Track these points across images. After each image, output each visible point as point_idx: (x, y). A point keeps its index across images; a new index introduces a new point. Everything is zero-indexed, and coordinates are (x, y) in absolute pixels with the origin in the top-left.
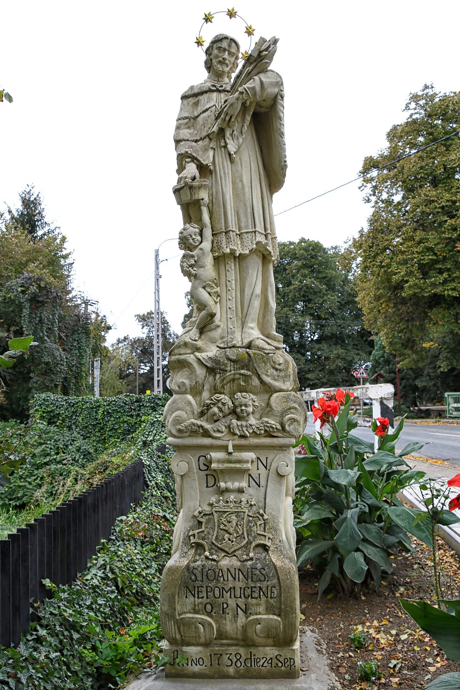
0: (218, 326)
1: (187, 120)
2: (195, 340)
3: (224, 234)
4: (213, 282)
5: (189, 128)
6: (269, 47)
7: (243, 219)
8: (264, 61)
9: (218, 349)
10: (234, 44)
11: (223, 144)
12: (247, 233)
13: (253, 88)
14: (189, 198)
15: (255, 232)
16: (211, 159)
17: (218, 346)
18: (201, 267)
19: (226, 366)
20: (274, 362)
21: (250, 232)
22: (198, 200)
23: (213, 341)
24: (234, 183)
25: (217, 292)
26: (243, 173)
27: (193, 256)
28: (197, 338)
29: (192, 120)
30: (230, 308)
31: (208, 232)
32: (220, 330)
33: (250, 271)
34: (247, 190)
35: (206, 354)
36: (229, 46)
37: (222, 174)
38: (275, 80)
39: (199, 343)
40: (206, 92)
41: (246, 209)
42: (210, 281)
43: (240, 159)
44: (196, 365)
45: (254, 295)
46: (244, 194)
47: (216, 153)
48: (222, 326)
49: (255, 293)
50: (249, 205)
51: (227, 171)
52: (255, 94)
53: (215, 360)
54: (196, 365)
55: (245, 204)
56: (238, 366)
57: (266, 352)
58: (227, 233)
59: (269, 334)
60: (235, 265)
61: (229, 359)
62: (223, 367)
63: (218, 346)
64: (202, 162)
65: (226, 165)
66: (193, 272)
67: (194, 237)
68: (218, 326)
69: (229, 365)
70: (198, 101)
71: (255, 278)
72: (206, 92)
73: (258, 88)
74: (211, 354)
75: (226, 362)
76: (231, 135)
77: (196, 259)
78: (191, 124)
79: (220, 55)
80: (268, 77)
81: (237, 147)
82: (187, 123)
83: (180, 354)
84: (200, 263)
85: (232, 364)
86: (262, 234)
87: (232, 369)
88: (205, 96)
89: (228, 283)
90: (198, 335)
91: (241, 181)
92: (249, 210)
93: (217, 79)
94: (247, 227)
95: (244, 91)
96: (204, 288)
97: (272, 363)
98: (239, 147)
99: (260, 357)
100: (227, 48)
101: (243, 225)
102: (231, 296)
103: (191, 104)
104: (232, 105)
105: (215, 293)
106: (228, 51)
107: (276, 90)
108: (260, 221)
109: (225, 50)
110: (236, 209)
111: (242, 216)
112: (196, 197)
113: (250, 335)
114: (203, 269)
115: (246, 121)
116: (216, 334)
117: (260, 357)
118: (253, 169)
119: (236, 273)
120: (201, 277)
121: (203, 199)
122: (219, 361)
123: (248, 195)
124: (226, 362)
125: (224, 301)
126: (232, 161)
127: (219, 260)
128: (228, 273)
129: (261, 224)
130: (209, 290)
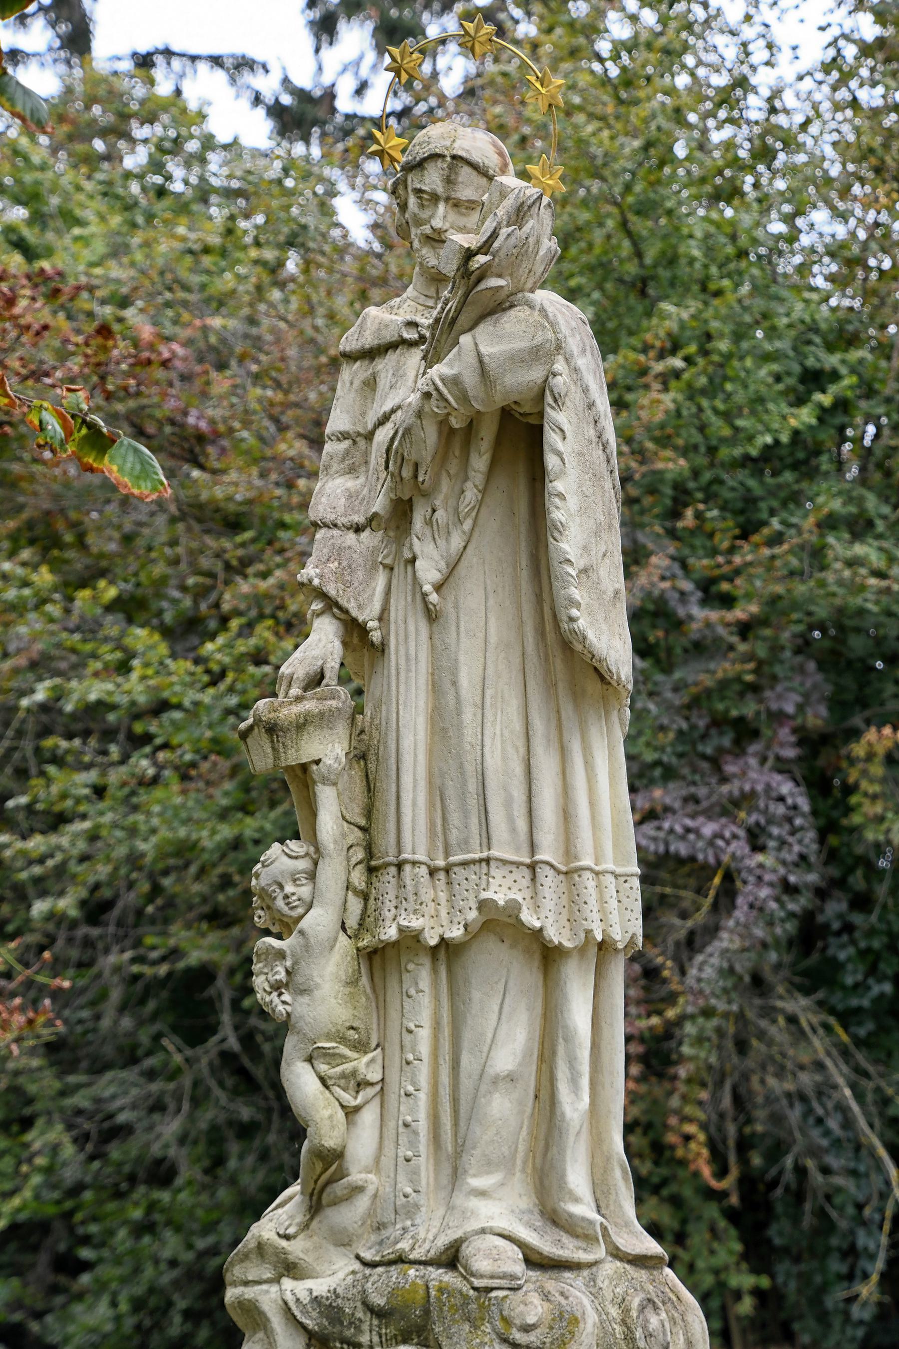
0: (358, 1189)
1: (346, 444)
2: (287, 1237)
3: (393, 870)
4: (343, 1040)
5: (352, 470)
6: (494, 235)
7: (455, 818)
8: (482, 286)
9: (357, 1266)
10: (466, 171)
11: (407, 555)
12: (465, 864)
13: (454, 382)
14: (270, 761)
15: (488, 861)
16: (376, 606)
17: (358, 1257)
18: (303, 991)
19: (358, 1329)
20: (507, 1321)
21: (474, 862)
22: (304, 767)
23: (342, 1240)
24: (436, 689)
25: (354, 1073)
26: (462, 658)
27: (281, 955)
28: (291, 1231)
29: (362, 442)
30: (406, 1125)
31: (332, 873)
32: (362, 1203)
33: (476, 995)
34: (468, 715)
35: (309, 1283)
36: (449, 181)
37: (402, 662)
38: (524, 344)
39: (296, 1249)
40: (392, 346)
41: (464, 783)
42: (329, 1037)
43: (456, 607)
44: (277, 1322)
45: (487, 1079)
46: (460, 726)
47: (394, 582)
48: (371, 1190)
49: (491, 1071)
50: (470, 768)
51: (412, 651)
52: (464, 398)
53: (328, 1307)
54: (277, 1322)
55: (461, 767)
56: (391, 1331)
57: (477, 1283)
58: (399, 866)
59: (554, 1211)
60: (435, 970)
61: (369, 1308)
62: (349, 1332)
63: (358, 1257)
64: (354, 613)
65: (412, 628)
66: (281, 1008)
67: (289, 888)
68: (358, 1189)
69: (365, 1327)
70: (374, 376)
71: (495, 1017)
72: (392, 346)
73: (471, 380)
74: (320, 1286)
75: (360, 1314)
76: (429, 522)
77: (289, 963)
78: (358, 457)
79: (425, 215)
80: (500, 338)
81: (442, 565)
82: (347, 453)
83: (246, 1283)
84: (299, 979)
85: (375, 1322)
86: (518, 864)
87: (376, 1339)
88: (392, 357)
89: (407, 1038)
90: (299, 1219)
91: (454, 683)
92: (472, 786)
93: (432, 292)
94: (465, 844)
95: (431, 389)
96: (310, 1060)
97: (499, 1324)
98: (453, 567)
99: (458, 1301)
100: (440, 190)
101: (454, 835)
102: (413, 1083)
103: (357, 383)
104: (408, 431)
105: (343, 1076)
106: (447, 199)
107: (536, 374)
108: (511, 820)
109: (435, 198)
110: (438, 781)
111: (452, 805)
112: (292, 758)
113: (466, 1214)
114: (305, 999)
115: (472, 474)
116: (350, 1215)
117: (458, 1301)
118: (493, 639)
119: (437, 998)
120: (301, 1024)
121: (318, 762)
122: (340, 1309)
123: (470, 734)
124: (360, 1314)
125: (392, 1098)
126: (432, 615)
127: (380, 961)
128: (407, 1003)
129: (513, 830)
130: (323, 1068)
